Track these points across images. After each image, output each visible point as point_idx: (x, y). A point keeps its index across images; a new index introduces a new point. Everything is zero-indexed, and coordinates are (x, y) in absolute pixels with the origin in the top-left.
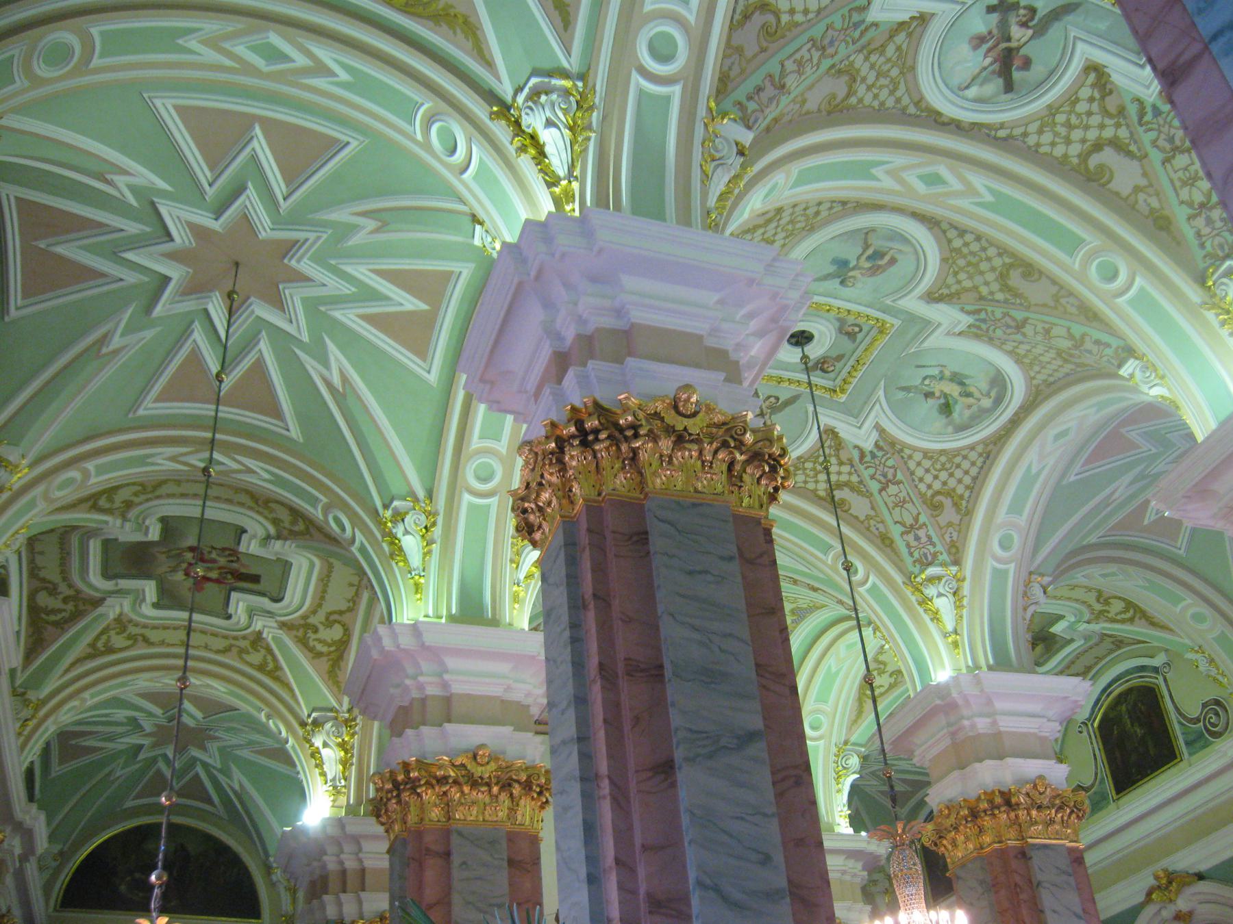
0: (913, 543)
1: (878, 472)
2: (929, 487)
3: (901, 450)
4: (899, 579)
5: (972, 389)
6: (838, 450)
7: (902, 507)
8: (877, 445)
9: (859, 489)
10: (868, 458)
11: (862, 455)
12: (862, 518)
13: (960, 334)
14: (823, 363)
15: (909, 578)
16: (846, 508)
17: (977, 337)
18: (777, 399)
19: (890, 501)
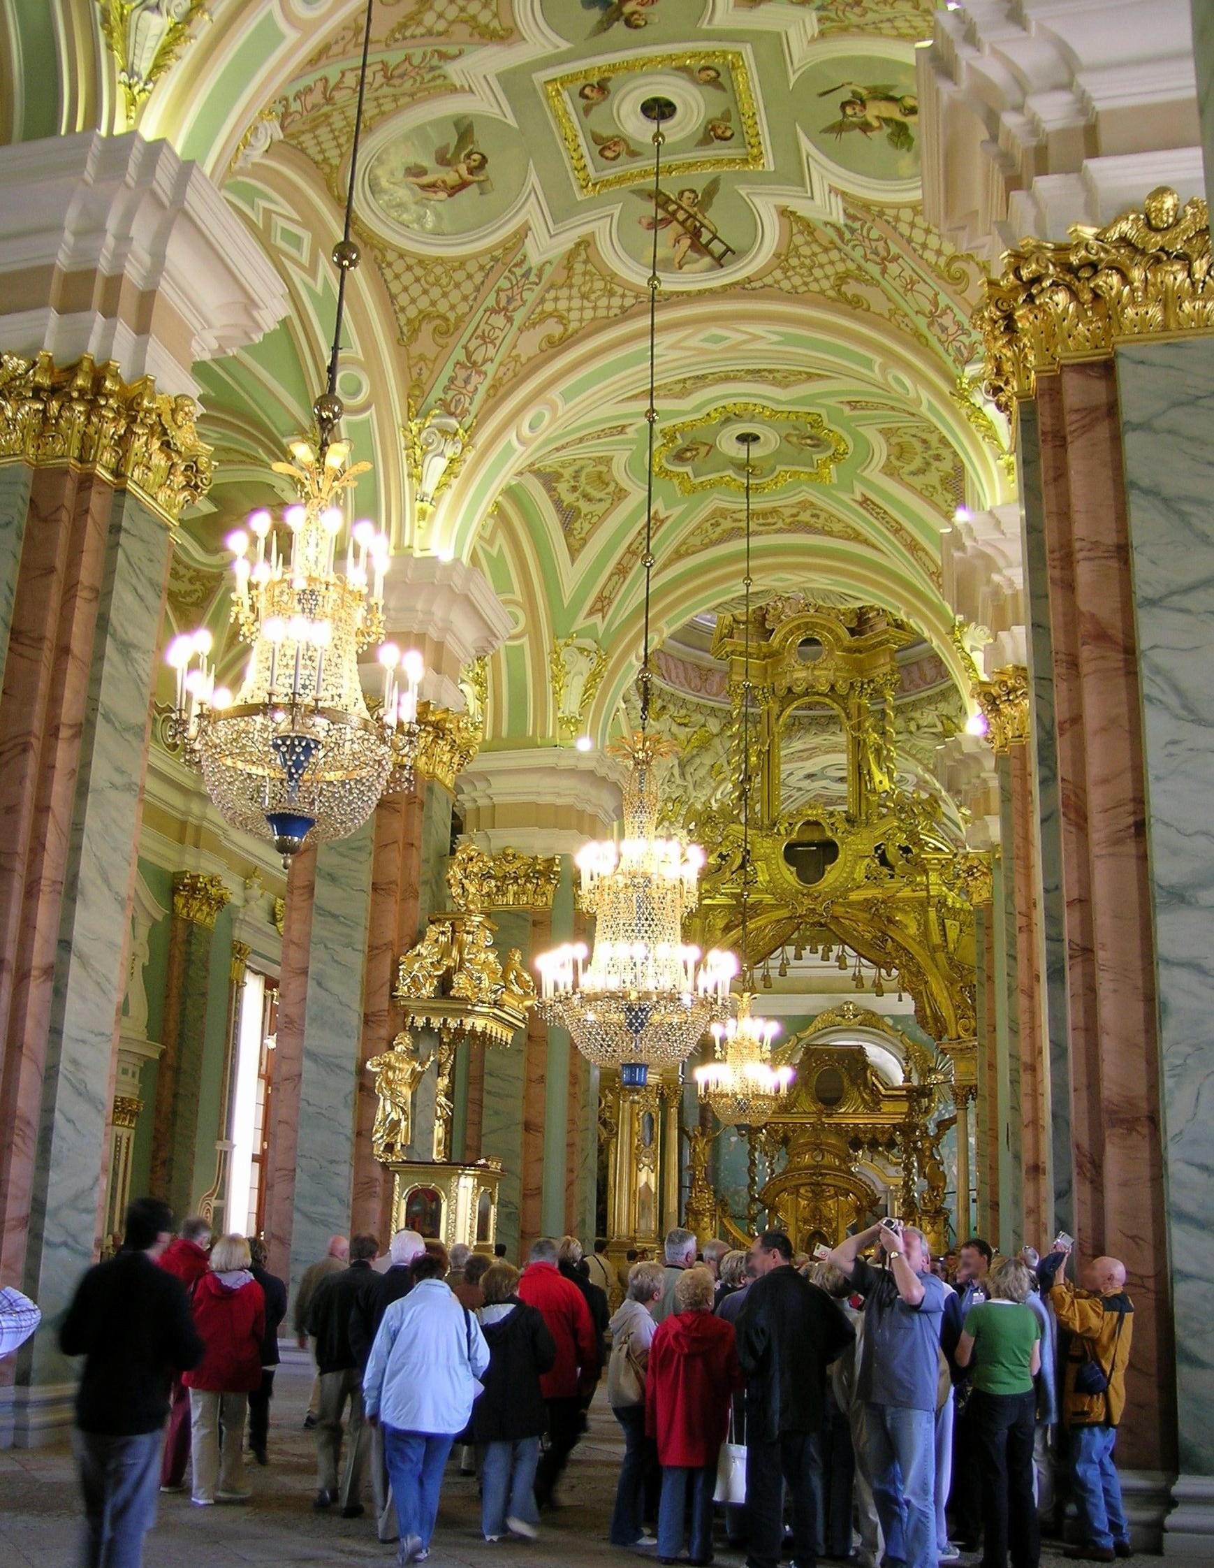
0: (944, 337)
1: (868, 251)
2: (939, 253)
3: (881, 214)
4: (946, 389)
5: (910, 102)
6: (811, 233)
7: (911, 289)
8: (847, 215)
9: (860, 276)
10: (847, 236)
11: (837, 229)
12: (887, 315)
13: (822, 34)
14: (713, 129)
15: (951, 380)
16: (865, 306)
17: (844, 30)
18: (693, 191)
19: (897, 283)
